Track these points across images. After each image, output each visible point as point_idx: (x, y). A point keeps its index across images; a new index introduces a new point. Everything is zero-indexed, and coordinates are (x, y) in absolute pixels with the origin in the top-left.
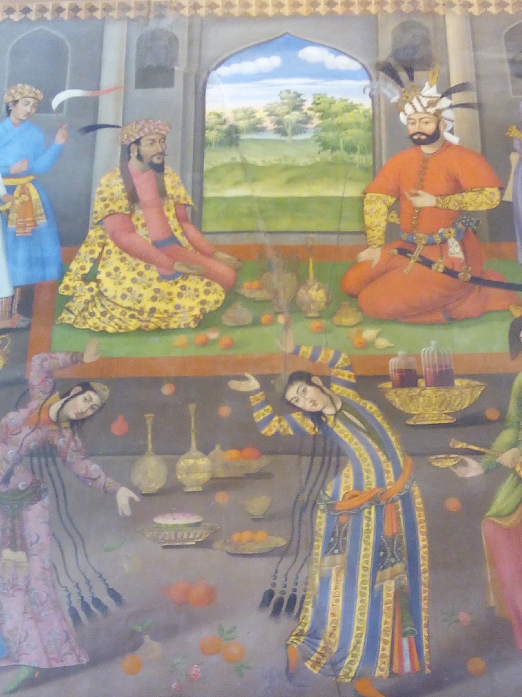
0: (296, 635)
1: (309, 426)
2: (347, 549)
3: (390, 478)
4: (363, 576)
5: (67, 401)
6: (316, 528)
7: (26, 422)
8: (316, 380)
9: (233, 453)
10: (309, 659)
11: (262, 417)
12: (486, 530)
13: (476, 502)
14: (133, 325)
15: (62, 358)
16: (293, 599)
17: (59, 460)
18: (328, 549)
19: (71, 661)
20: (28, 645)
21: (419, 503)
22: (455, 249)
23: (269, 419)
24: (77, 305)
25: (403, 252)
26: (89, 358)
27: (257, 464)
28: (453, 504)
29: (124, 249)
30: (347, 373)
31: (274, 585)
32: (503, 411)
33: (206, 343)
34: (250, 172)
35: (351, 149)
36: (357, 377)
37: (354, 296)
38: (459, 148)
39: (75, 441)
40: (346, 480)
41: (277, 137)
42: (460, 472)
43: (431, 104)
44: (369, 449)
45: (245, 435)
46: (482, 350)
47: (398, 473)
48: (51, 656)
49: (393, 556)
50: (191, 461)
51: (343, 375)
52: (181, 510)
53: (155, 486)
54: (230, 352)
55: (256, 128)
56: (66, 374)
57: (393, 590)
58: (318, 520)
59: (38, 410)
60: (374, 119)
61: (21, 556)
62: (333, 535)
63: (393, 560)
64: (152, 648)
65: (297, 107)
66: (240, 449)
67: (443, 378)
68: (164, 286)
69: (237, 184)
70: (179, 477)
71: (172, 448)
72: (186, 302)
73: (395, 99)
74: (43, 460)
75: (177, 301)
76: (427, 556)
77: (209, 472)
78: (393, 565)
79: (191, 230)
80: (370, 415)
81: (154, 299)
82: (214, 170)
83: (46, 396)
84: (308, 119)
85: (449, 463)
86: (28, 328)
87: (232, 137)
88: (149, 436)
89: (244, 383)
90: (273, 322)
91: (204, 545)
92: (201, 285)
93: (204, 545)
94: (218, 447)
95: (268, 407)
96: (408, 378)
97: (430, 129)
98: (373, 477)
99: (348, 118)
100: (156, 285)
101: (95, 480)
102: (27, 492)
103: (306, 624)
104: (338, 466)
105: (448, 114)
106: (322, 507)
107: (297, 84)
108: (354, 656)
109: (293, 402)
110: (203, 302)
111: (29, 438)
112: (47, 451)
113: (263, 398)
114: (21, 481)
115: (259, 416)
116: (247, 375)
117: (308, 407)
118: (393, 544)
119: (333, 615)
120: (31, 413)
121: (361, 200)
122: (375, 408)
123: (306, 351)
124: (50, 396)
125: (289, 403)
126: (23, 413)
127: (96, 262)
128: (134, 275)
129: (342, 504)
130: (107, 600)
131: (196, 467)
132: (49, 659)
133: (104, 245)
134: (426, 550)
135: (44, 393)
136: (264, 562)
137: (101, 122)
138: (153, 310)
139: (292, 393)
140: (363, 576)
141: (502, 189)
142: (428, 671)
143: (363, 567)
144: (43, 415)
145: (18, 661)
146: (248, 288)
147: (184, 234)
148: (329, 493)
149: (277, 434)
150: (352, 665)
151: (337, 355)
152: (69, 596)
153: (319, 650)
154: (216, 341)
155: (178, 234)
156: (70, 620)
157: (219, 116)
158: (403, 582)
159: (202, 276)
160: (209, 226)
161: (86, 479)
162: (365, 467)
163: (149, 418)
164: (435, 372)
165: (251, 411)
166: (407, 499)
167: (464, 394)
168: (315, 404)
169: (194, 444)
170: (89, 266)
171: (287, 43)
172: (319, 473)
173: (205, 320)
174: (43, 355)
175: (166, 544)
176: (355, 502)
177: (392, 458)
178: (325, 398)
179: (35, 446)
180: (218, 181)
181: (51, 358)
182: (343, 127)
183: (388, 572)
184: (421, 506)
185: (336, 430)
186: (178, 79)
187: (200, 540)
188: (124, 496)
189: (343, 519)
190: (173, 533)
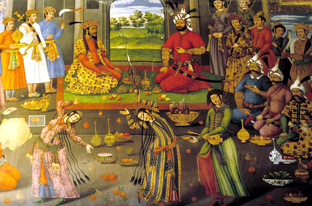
0: (141, 190)
1: (145, 126)
2: (157, 164)
3: (169, 143)
4: (161, 173)
5: (69, 117)
6: (147, 158)
7: (57, 123)
8: (147, 111)
9: (122, 134)
10: (145, 197)
11: (130, 123)
13: (196, 150)
16: (140, 179)
17: (68, 135)
18: (151, 164)
19: (75, 197)
20: (61, 192)
21: (178, 151)
22: (191, 68)
23: (133, 123)
24: (71, 85)
25: (174, 68)
26: (75, 103)
27: (129, 138)
28: (188, 151)
29: (85, 66)
30: (156, 109)
31: (135, 175)
32: (205, 122)
33: (112, 98)
34: (126, 40)
36: (159, 110)
37: (158, 83)
39: (72, 130)
40: (156, 143)
41: (133, 27)
42: (191, 141)
43: (184, 17)
44: (163, 133)
45: (125, 129)
46: (198, 102)
47: (172, 141)
48: (69, 195)
49: (170, 167)
50: (109, 137)
51: (155, 110)
52: (106, 152)
53: (98, 144)
54: (120, 102)
55: (127, 24)
56: (68, 108)
57: (170, 177)
58: (148, 155)
59: (60, 120)
61: (58, 165)
62: (153, 160)
63: (170, 168)
64: (98, 193)
65: (140, 17)
66: (124, 133)
69: (121, 44)
70: (105, 142)
72: (106, 85)
73: (172, 14)
74: (63, 135)
75: (103, 84)
76: (180, 167)
77: (114, 140)
78: (170, 169)
79: (106, 59)
80: (164, 123)
81: (95, 83)
82: (114, 38)
83: (63, 115)
85: (188, 138)
86: (56, 92)
87: (118, 27)
88: (96, 128)
89: (124, 112)
90: (133, 92)
91: (114, 162)
92: (110, 79)
94: (117, 132)
95: (132, 120)
97: (183, 25)
98: (164, 142)
99: (156, 21)
100: (96, 79)
101: (79, 142)
102: (59, 146)
103: (144, 187)
104: (154, 139)
105: (189, 20)
106: (149, 151)
107: (139, 8)
108: (158, 196)
109: (140, 118)
110: (111, 85)
111: (58, 128)
112: (63, 133)
113: (131, 117)
114: (56, 142)
115: (129, 122)
116: (125, 109)
117: (145, 120)
118: (170, 163)
119: (152, 184)
120: (58, 120)
121: (161, 50)
122: (165, 120)
123: (144, 101)
124: (64, 115)
125: (139, 118)
126: (56, 120)
128: (89, 75)
129: (155, 151)
130: (84, 179)
131: (110, 138)
132: (68, 196)
133: (79, 65)
134: (180, 165)
135: (62, 114)
136: (131, 168)
137: (76, 21)
138: (95, 87)
139: (140, 115)
140: (161, 173)
141: (206, 47)
142: (180, 200)
143: (161, 170)
144: (62, 121)
145: (59, 196)
146: (125, 81)
147: (104, 61)
148: (151, 147)
149: (135, 128)
150: (158, 198)
151: (154, 103)
152: (73, 177)
153: (148, 194)
154: (116, 97)
155: (102, 61)
156: (74, 184)
157: (115, 19)
158: (173, 174)
159: (110, 76)
161: (75, 142)
162: (162, 139)
164: (184, 109)
166: (175, 149)
167: (193, 116)
168: (147, 119)
169: (109, 131)
170: (74, 72)
172: (148, 141)
173: (112, 91)
174: (61, 102)
175: (102, 162)
176: (159, 150)
177: (170, 136)
178: (150, 117)
179: (60, 131)
180: (115, 43)
181: (64, 103)
182: (155, 24)
183: (169, 171)
184: (179, 151)
185: (153, 127)
186: (101, 7)
187: (112, 161)
188: (88, 147)
189: (155, 155)
190: (104, 159)
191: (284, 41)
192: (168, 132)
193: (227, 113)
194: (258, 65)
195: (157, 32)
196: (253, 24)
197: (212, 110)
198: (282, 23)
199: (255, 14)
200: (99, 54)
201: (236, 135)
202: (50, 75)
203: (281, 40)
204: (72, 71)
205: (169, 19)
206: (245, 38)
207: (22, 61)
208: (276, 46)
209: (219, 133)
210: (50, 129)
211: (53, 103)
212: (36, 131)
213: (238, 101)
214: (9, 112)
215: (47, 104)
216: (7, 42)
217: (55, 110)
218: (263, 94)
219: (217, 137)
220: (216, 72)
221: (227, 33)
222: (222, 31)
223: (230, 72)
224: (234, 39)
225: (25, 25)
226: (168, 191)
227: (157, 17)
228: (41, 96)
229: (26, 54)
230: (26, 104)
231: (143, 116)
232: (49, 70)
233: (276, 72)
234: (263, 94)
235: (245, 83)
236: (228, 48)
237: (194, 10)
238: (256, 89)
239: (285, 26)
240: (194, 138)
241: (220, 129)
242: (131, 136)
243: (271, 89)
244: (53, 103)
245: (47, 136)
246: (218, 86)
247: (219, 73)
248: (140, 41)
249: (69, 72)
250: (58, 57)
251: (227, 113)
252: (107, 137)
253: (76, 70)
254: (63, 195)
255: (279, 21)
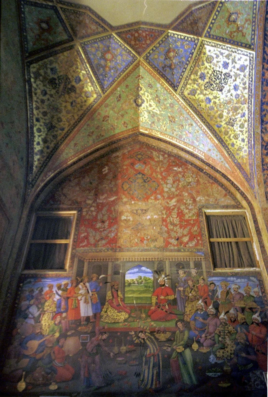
1: (142, 341)
3: (155, 351)
4: (151, 370)
9: (130, 346)
12: (171, 361)
14: (113, 321)
15: (101, 327)
18: (145, 364)
19: (103, 385)
22: (167, 307)
23: (136, 340)
24: (104, 317)
25: (159, 307)
26: (106, 328)
33: (125, 325)
34: (133, 292)
35: (149, 287)
37: (150, 316)
38: (168, 287)
41: (137, 285)
43: (164, 279)
47: (157, 350)
55: (134, 283)
60: (154, 281)
67: (164, 332)
68: (118, 314)
69: (131, 294)
71: (120, 345)
79: (123, 303)
84: (142, 281)
87: (130, 285)
91: (125, 364)
93: (125, 364)
96: (158, 332)
97: (163, 283)
99: (149, 281)
105: (166, 281)
107: (141, 274)
111: (96, 343)
112: (99, 345)
114: (95, 351)
115: (134, 339)
117: (142, 338)
123: (142, 327)
127: (107, 309)
129: (148, 356)
130: (109, 374)
131: (124, 349)
139: (139, 335)
140: (151, 370)
141: (175, 295)
150: (149, 386)
159: (125, 312)
160: (125, 302)
162: (152, 349)
163: (116, 339)
165: (133, 338)
166: (158, 355)
167: (168, 335)
171: (139, 266)
173: (125, 320)
177: (156, 347)
188: (112, 354)
191: (215, 292)
192: (155, 344)
193: (186, 333)
194: (202, 305)
195: (149, 287)
196: (199, 283)
197: (178, 332)
198: (214, 282)
199: (200, 278)
200: (119, 300)
201: (191, 346)
202: (93, 312)
203: (214, 290)
204: (104, 310)
205: (156, 280)
206: (195, 291)
207: (79, 303)
208: (210, 294)
209: (182, 345)
210: (92, 343)
211: (94, 327)
212: (84, 344)
213: (192, 327)
214: (70, 333)
215: (91, 328)
216: (72, 293)
217: (94, 332)
218: (205, 322)
219: (181, 347)
220: (180, 309)
221: (186, 288)
222: (183, 287)
223: (188, 310)
224: (189, 291)
225: (82, 284)
226: (154, 381)
227: (150, 279)
228: (87, 324)
229: (81, 299)
230: (79, 328)
231: (141, 335)
232: (93, 309)
233: (212, 309)
234: (205, 322)
235: (195, 316)
236: (186, 296)
237: (168, 275)
238: (201, 320)
239: (216, 283)
240: (169, 348)
241: (182, 342)
242: (135, 348)
243: (209, 318)
244: (94, 327)
245: (90, 347)
246: (181, 317)
247: (182, 310)
248: (141, 292)
249: (103, 310)
250: (98, 301)
251: (186, 333)
252: (122, 348)
253: (107, 309)
254: (97, 385)
255: (213, 281)
